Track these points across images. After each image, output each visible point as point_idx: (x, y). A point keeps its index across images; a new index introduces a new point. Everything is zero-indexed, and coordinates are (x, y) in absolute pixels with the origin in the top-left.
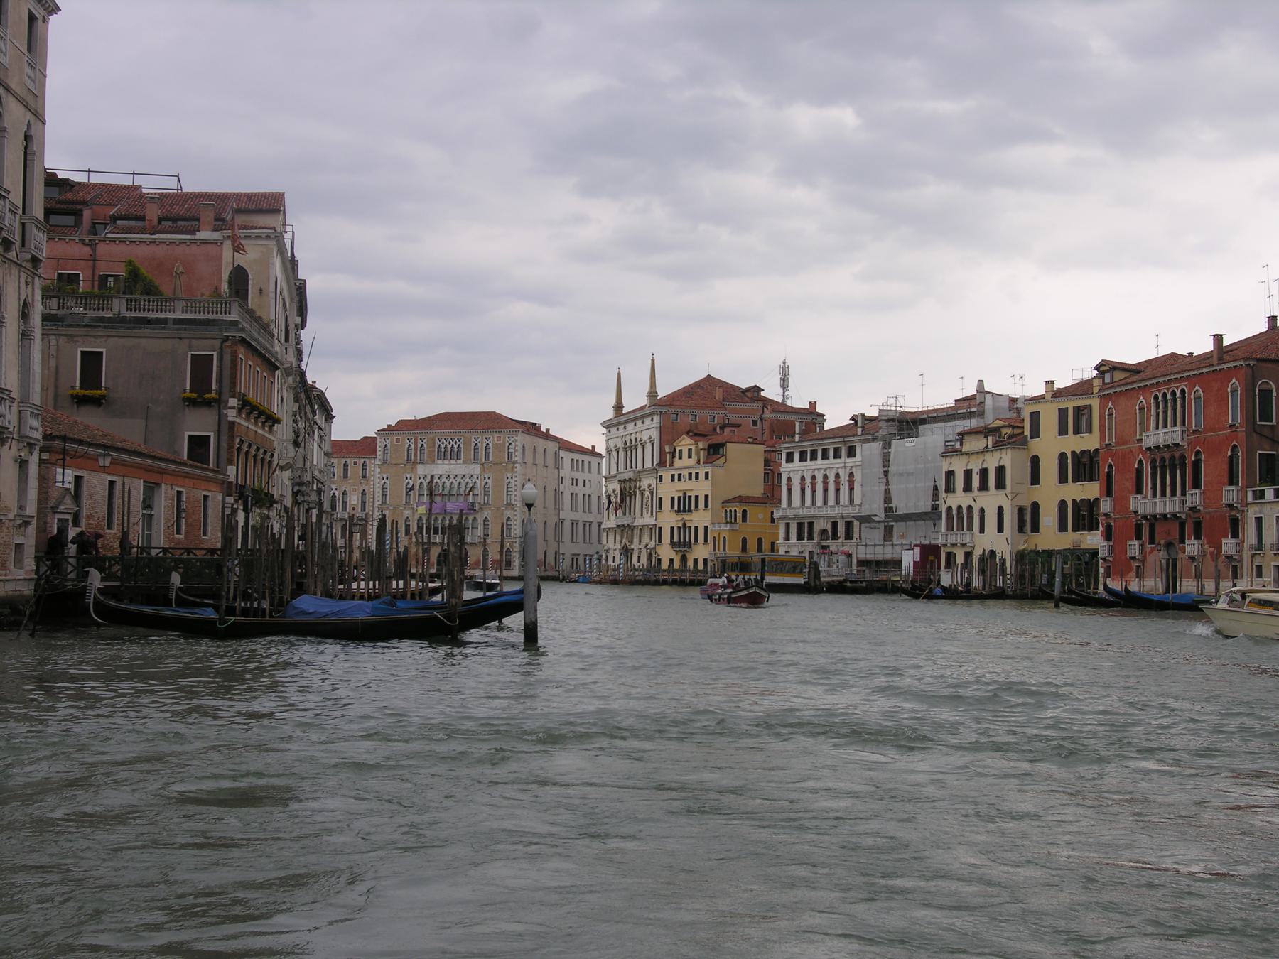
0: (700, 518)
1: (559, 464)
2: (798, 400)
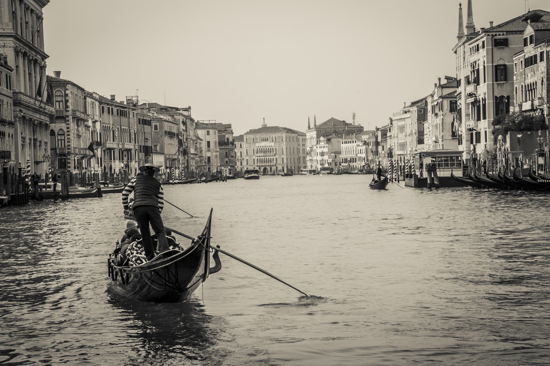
0: (326, 157)
1: (298, 140)
2: (356, 124)
